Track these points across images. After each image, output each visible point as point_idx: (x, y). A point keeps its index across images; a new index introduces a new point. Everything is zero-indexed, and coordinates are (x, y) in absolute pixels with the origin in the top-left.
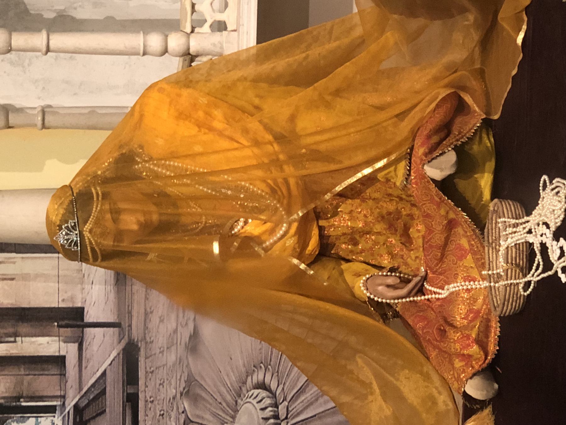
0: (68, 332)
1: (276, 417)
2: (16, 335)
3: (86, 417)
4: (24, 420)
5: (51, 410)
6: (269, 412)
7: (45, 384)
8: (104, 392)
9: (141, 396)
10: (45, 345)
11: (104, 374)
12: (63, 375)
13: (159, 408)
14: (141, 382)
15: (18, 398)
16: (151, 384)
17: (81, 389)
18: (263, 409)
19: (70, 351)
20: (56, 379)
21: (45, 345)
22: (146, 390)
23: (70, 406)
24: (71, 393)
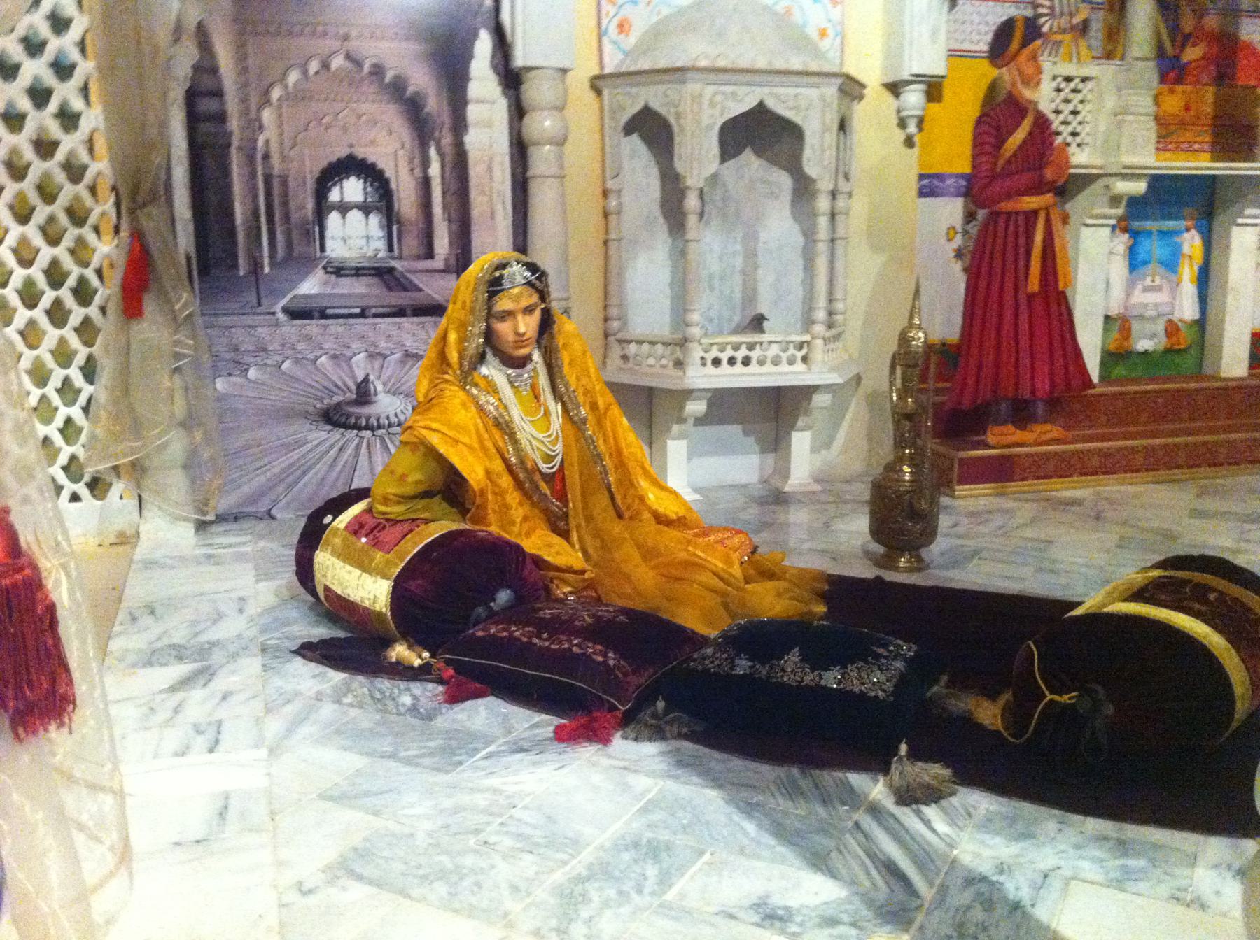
0: (453, 261)
1: (390, 425)
2: (449, 221)
3: (386, 277)
4: (382, 227)
5: (390, 249)
6: (394, 419)
7: (412, 243)
8: (406, 289)
9: (404, 319)
10: (442, 243)
11: (421, 290)
12: (419, 258)
13: (395, 333)
14: (415, 319)
15: (399, 222)
16: (414, 327)
17: (410, 271)
18: (388, 418)
19: (438, 263)
20: (415, 252)
21: (442, 243)
22: (408, 323)
23: (393, 263)
24: (405, 263)
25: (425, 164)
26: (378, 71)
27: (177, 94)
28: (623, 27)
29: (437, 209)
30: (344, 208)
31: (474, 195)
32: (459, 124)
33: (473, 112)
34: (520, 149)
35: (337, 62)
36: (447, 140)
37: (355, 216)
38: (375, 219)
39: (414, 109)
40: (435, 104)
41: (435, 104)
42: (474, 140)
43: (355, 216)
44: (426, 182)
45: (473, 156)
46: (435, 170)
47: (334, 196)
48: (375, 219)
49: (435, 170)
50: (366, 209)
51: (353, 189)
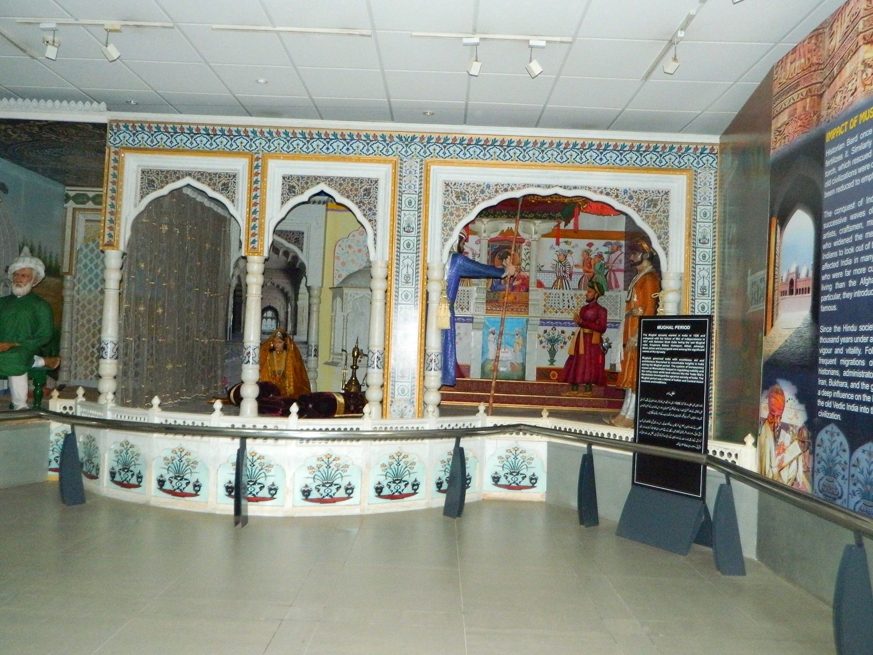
25: (287, 308)
26: (278, 286)
27: (232, 290)
28: (339, 276)
29: (289, 319)
30: (267, 318)
31: (299, 316)
32: (296, 299)
33: (300, 296)
34: (310, 305)
35: (269, 284)
36: (293, 302)
37: (269, 320)
38: (274, 321)
39: (286, 296)
40: (291, 294)
41: (291, 294)
42: (299, 303)
43: (269, 320)
44: (287, 313)
45: (299, 306)
46: (289, 309)
47: (265, 315)
48: (274, 321)
49: (289, 309)
50: (272, 318)
51: (269, 314)
